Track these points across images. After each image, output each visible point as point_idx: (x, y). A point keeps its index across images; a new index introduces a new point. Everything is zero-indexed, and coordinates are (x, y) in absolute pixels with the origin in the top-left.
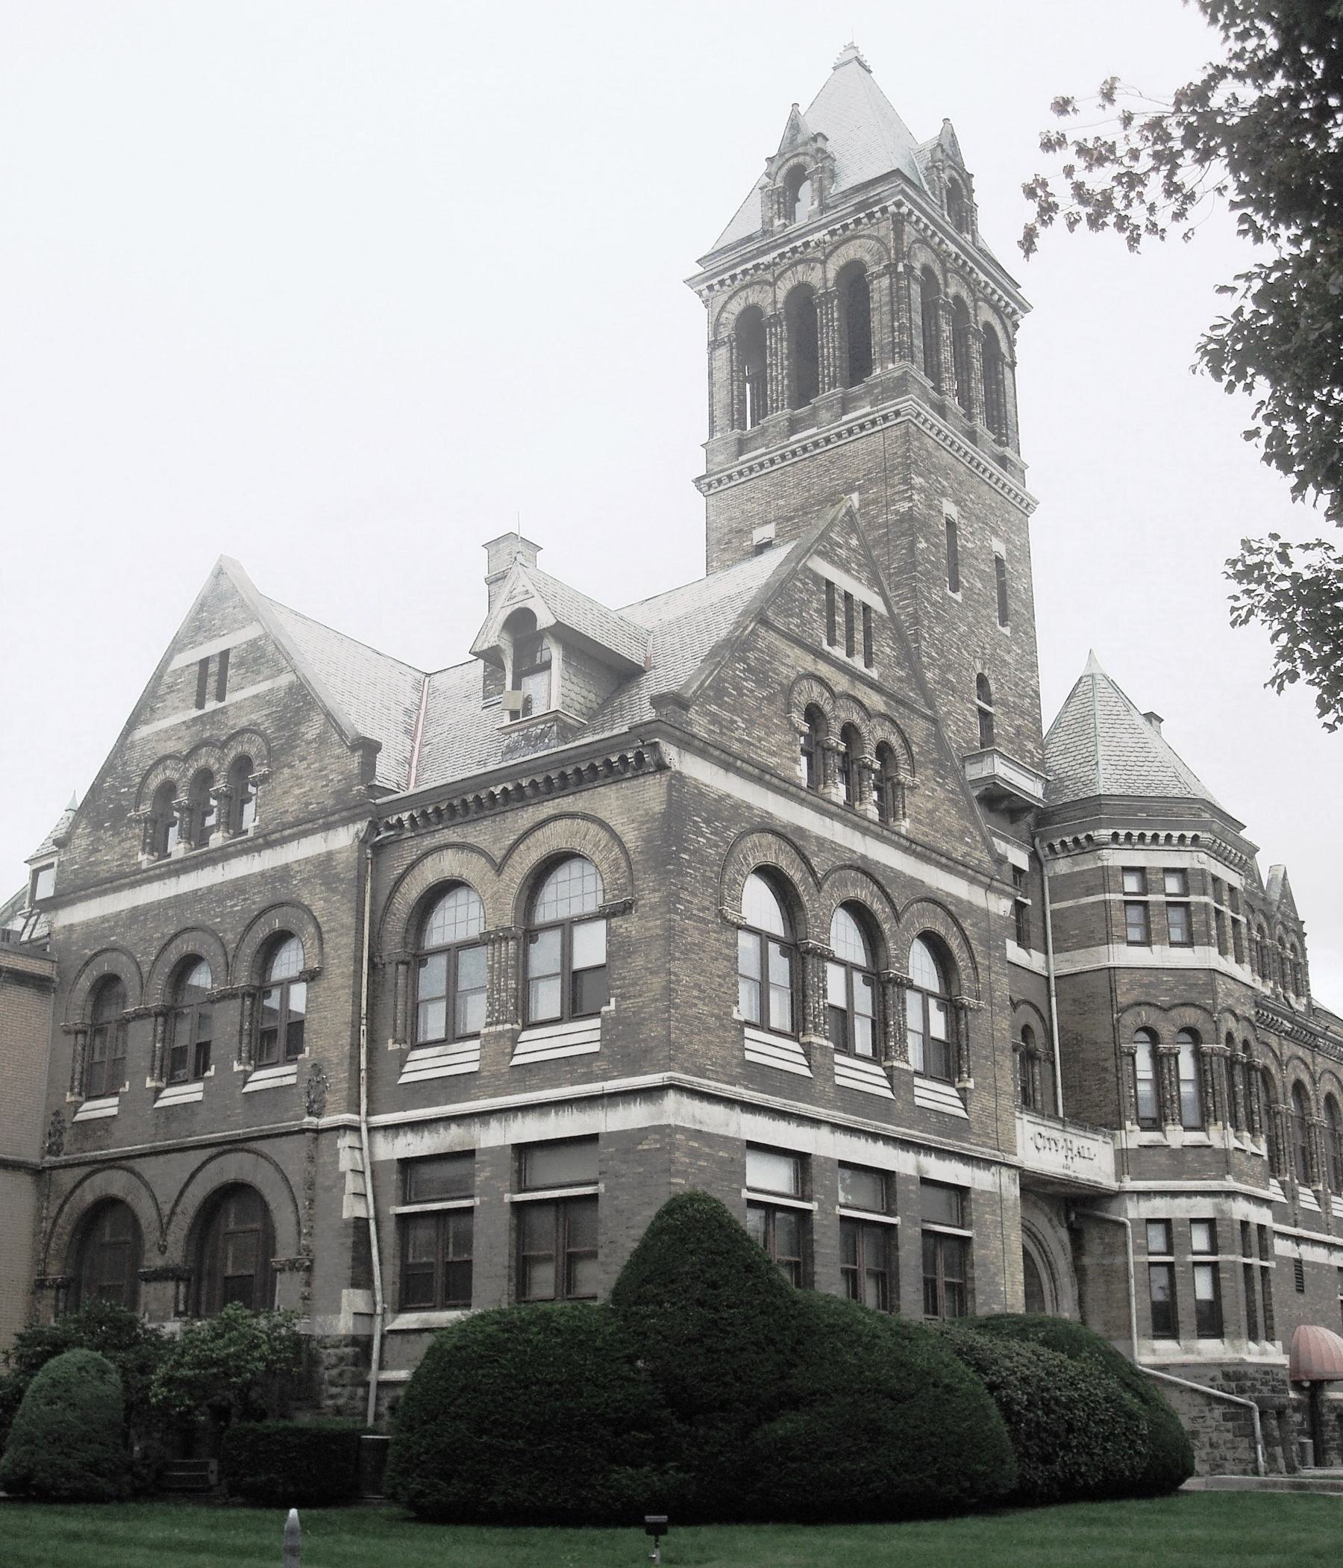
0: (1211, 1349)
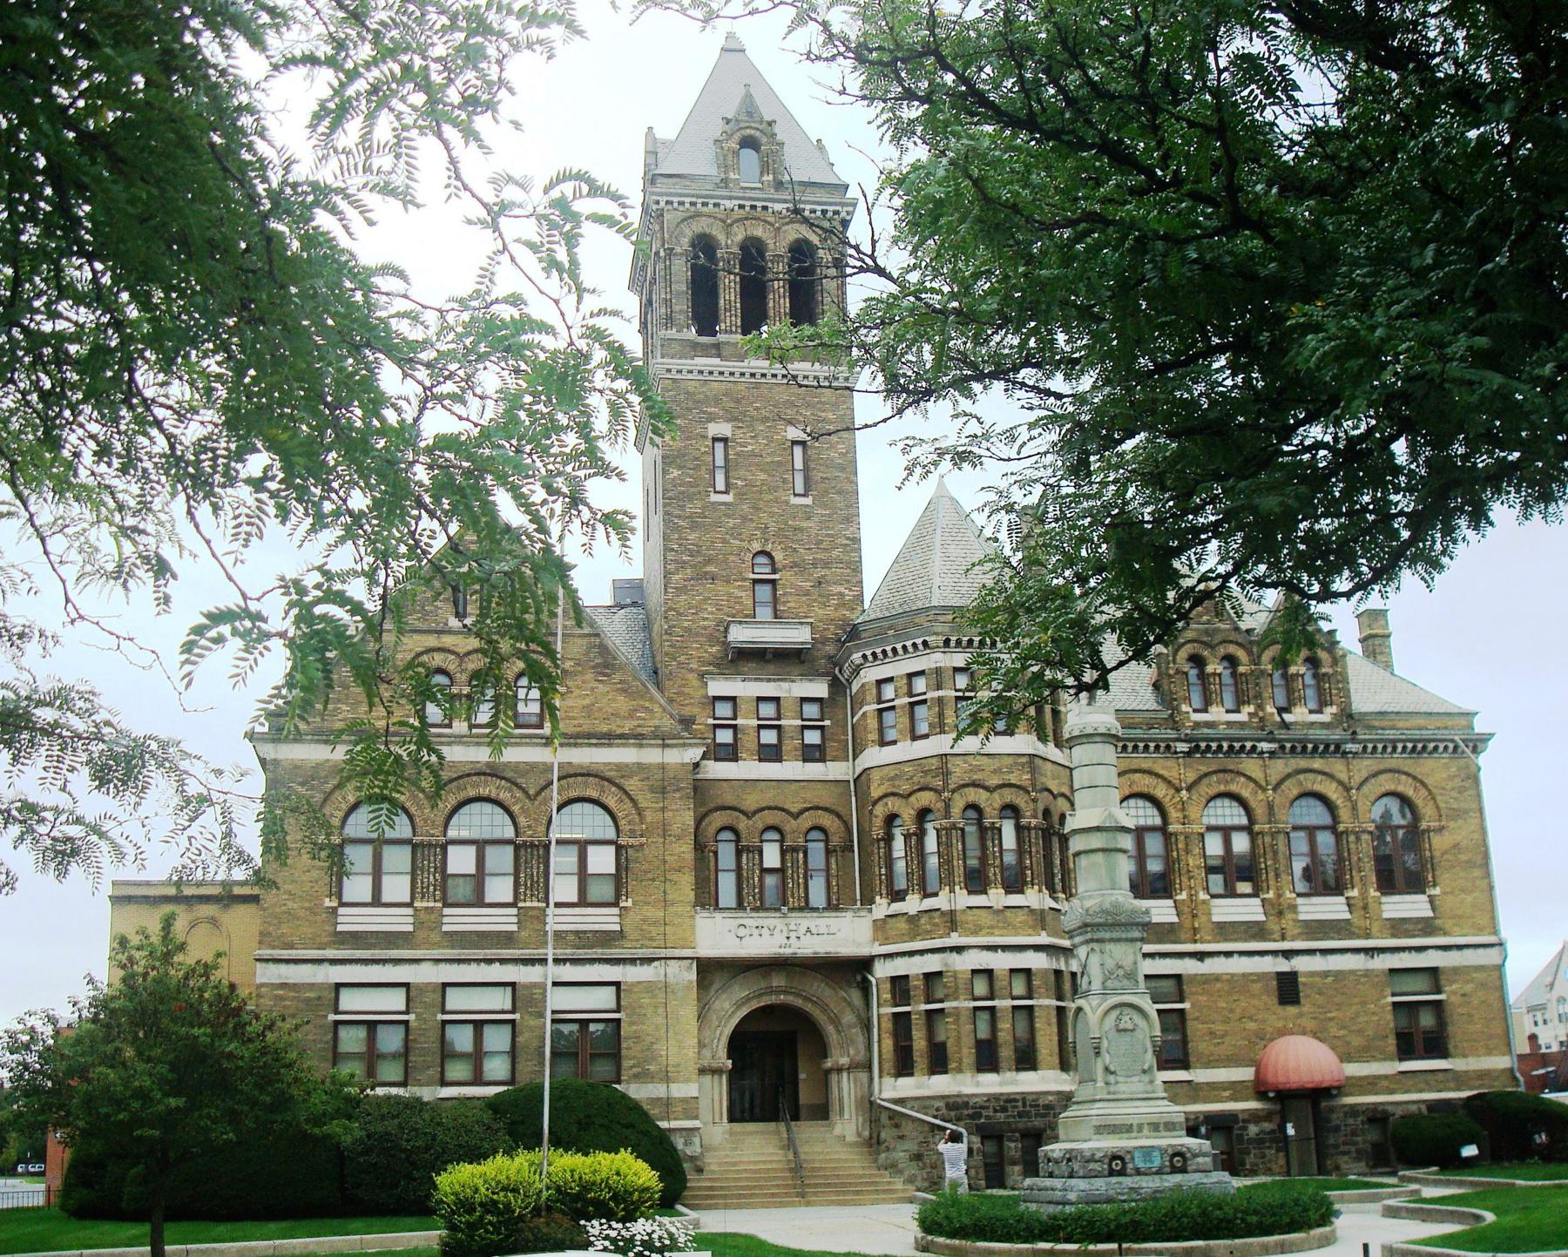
0: (941, 1085)
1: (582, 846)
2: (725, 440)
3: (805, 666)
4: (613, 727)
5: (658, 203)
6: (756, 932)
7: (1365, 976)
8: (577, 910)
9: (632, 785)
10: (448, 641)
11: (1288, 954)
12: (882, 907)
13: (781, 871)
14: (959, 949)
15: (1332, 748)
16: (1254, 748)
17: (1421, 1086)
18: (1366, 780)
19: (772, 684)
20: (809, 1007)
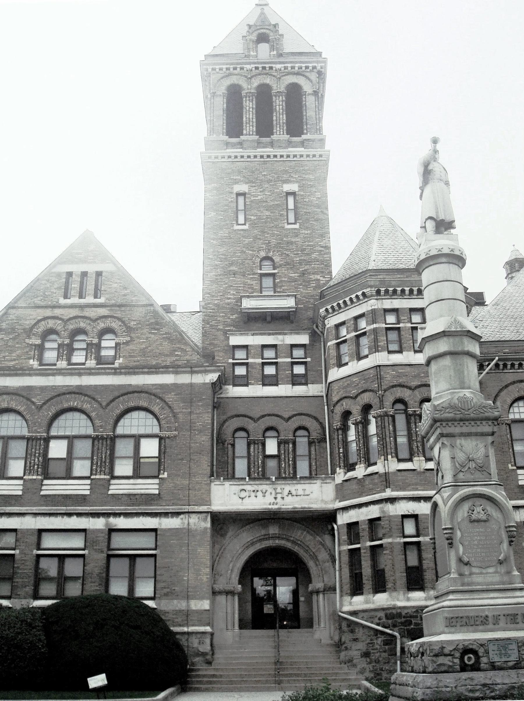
0: (382, 600)
1: (137, 439)
2: (244, 194)
3: (293, 325)
4: (160, 361)
5: (207, 70)
6: (253, 494)
8: (132, 481)
9: (170, 398)
12: (341, 476)
13: (277, 457)
14: (392, 500)
19: (272, 337)
20: (296, 549)
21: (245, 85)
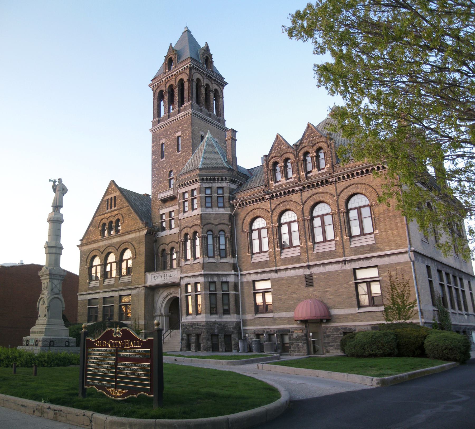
7: (342, 273)
8: (126, 277)
9: (134, 243)
10: (106, 215)
11: (309, 267)
15: (324, 181)
16: (293, 190)
17: (369, 318)
18: (342, 191)
21: (164, 89)
